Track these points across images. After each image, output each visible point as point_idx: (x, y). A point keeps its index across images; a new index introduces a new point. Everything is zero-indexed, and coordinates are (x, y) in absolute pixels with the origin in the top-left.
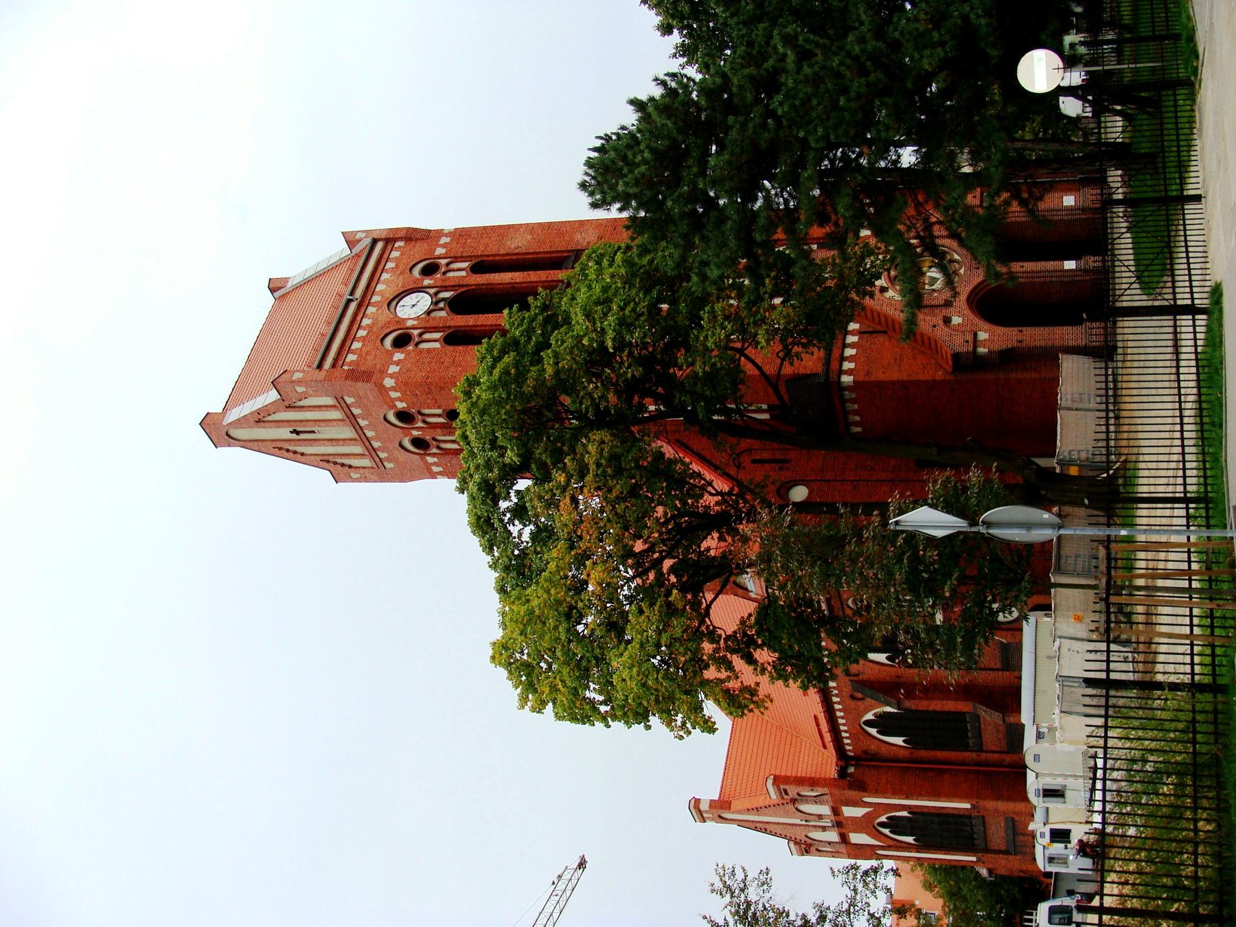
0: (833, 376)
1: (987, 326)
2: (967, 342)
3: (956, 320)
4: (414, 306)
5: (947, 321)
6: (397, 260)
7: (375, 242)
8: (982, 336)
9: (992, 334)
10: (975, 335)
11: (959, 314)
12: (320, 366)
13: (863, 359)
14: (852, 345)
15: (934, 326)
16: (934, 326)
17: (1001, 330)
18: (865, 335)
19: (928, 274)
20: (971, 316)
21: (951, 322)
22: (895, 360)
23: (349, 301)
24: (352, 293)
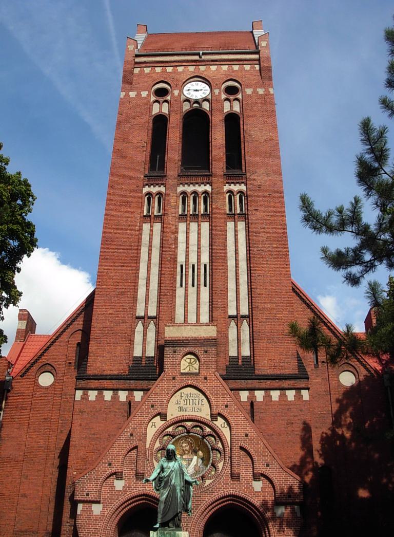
0: (83, 383)
1: (108, 513)
2: (88, 495)
3: (119, 485)
4: (197, 90)
5: (118, 475)
7: (258, 53)
8: (97, 509)
9: (97, 519)
10: (98, 502)
11: (127, 487)
12: (137, 56)
13: (97, 406)
14: (115, 397)
15: (110, 464)
16: (110, 464)
18: (126, 407)
19: (195, 458)
20: (122, 499)
21: (117, 479)
22: (94, 434)
23: (198, 54)
24: (203, 54)
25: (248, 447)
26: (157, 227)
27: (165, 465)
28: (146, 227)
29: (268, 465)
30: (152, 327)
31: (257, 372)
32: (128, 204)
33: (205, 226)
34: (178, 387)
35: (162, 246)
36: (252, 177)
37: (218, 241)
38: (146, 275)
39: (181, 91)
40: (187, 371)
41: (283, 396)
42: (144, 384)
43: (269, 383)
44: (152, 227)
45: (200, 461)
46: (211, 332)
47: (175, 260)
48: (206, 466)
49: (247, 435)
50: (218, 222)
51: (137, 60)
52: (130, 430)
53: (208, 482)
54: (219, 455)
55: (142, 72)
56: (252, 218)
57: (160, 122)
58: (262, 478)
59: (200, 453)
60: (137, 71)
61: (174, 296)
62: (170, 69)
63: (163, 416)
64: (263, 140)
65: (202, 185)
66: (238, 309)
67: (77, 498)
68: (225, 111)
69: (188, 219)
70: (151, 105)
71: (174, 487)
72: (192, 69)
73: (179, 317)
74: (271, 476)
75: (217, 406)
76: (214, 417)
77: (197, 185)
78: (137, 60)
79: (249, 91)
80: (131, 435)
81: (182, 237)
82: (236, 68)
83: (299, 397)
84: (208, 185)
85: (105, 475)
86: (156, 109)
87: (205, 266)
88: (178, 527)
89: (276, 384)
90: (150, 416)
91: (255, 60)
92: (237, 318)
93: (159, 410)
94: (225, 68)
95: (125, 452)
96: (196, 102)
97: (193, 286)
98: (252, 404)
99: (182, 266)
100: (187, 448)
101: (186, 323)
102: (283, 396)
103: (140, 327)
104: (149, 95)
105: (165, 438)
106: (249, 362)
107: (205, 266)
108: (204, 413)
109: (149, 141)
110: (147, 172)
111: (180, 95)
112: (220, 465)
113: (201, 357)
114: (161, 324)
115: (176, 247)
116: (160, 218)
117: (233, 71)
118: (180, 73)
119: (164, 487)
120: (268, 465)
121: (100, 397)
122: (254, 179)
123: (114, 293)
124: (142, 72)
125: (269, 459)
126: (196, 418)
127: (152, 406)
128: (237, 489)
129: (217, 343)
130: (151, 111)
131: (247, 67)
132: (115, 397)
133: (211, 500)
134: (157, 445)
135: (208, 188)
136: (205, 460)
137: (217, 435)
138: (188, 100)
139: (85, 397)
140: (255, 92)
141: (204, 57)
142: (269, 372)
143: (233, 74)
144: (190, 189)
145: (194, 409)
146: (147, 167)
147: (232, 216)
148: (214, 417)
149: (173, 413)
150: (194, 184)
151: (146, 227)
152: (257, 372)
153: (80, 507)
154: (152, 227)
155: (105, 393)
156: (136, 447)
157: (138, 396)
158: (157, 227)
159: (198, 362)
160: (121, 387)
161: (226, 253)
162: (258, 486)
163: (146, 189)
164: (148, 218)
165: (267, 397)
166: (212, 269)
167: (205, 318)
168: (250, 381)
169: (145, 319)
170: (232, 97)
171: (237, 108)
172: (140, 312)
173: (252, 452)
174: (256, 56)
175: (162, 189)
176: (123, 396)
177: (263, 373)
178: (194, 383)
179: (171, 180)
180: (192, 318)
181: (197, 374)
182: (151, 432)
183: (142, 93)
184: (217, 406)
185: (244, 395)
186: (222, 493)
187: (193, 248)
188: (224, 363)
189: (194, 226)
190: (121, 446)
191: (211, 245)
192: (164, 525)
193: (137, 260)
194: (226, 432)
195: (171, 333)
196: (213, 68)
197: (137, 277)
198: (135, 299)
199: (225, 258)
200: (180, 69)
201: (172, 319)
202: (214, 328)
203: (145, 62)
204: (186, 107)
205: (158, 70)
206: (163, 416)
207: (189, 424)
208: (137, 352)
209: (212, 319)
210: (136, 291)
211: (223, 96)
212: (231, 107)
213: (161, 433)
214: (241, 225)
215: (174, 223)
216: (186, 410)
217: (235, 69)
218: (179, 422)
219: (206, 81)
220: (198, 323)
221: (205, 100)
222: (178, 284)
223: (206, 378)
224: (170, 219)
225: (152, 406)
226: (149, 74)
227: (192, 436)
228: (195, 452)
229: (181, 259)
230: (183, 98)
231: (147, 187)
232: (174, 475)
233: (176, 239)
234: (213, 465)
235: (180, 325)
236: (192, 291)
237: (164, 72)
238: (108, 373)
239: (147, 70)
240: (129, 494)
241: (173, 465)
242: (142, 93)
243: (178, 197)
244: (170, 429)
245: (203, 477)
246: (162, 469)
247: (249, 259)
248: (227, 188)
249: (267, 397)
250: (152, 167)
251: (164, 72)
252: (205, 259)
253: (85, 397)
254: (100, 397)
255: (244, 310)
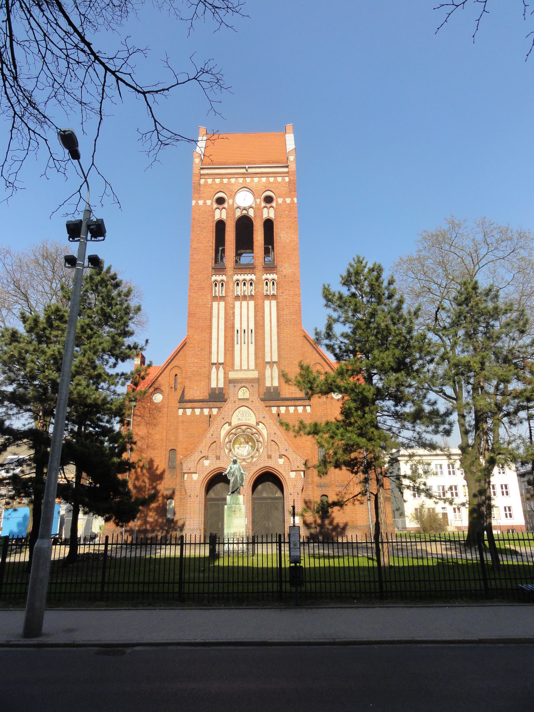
0: (183, 405)
1: (201, 478)
2: (190, 469)
3: (207, 463)
5: (206, 458)
6: (275, 182)
7: (287, 167)
8: (195, 477)
9: (195, 482)
10: (196, 473)
12: (202, 168)
13: (192, 418)
14: (202, 413)
15: (201, 452)
16: (201, 452)
17: (198, 486)
19: (247, 446)
24: (248, 168)
25: (276, 440)
26: (222, 304)
27: (232, 466)
28: (215, 304)
29: (286, 450)
30: (221, 369)
31: (281, 396)
32: (203, 289)
33: (252, 303)
34: (238, 407)
35: (225, 318)
36: (281, 270)
37: (260, 314)
38: (216, 337)
39: (234, 200)
40: (242, 397)
41: (296, 410)
42: (218, 404)
43: (288, 403)
44: (219, 304)
45: (250, 448)
46: (255, 375)
47: (233, 327)
48: (254, 450)
49: (275, 434)
50: (260, 301)
51: (203, 172)
52: (211, 432)
53: (255, 459)
54: (260, 445)
55: (206, 182)
56: (280, 299)
57: (220, 226)
58: (283, 457)
59: (250, 443)
60: (202, 181)
61: (233, 351)
62: (225, 181)
63: (230, 424)
64: (288, 241)
65: (249, 275)
66: (271, 359)
67: (184, 471)
68: (264, 217)
69: (241, 299)
70: (214, 212)
71: (237, 476)
72: (241, 180)
73: (237, 366)
74: (288, 456)
75: (259, 417)
76: (258, 424)
77: (246, 275)
78: (203, 172)
79: (280, 201)
80: (212, 435)
81: (237, 311)
82: (272, 180)
83: (305, 410)
84: (253, 275)
85: (199, 458)
86: (217, 217)
87: (252, 330)
88: (239, 493)
89: (292, 403)
90: (222, 424)
91: (285, 173)
92: (271, 363)
93: (227, 421)
94: (264, 180)
95: (209, 445)
96: (245, 209)
97: (245, 343)
98: (279, 415)
99: (238, 331)
100: (243, 441)
101: (241, 370)
102: (296, 410)
103: (214, 369)
104: (212, 204)
105: (231, 436)
106: (276, 390)
107: (252, 330)
108: (253, 421)
109: (214, 242)
110: (213, 265)
111: (233, 204)
112: (261, 450)
113: (250, 389)
114: (228, 368)
115: (234, 318)
116: (222, 298)
117: (270, 183)
118: (233, 184)
119: (232, 476)
120: (286, 450)
121: (193, 413)
122: (282, 271)
123: (197, 349)
124: (206, 182)
125: (287, 447)
126: (246, 424)
127: (223, 418)
128: (270, 463)
129: (259, 381)
130: (214, 217)
131: (279, 179)
132: (202, 413)
133: (256, 469)
134: (227, 440)
135: (253, 277)
136: (253, 447)
137: (259, 433)
138: (238, 207)
139: (184, 413)
140: (284, 202)
141: (250, 171)
142: (288, 396)
143: (270, 186)
144: (241, 277)
145: (246, 419)
146: (214, 261)
147: (267, 296)
148: (258, 424)
149: (235, 422)
150: (244, 274)
151: (215, 304)
152: (281, 396)
153: (186, 476)
154: (219, 304)
155: (196, 410)
156: (215, 442)
157: (215, 411)
158: (222, 304)
159: (248, 392)
160: (205, 406)
161: (264, 322)
162: (281, 461)
163: (214, 278)
164: (215, 298)
165: (287, 411)
166: (255, 333)
167: (252, 366)
168: (277, 402)
169: (217, 365)
170: (268, 205)
171: (272, 216)
172: (214, 360)
173: (278, 443)
174: (286, 170)
175: (224, 278)
176: (206, 411)
177: (285, 397)
178: (246, 405)
179: (230, 271)
180: (245, 367)
181: (247, 399)
182: (223, 432)
183: (207, 201)
184: (259, 417)
185: (274, 410)
186: (262, 465)
187: (244, 319)
188: (262, 391)
189: (244, 303)
190: (207, 440)
191: (255, 317)
192: (233, 493)
193: (210, 327)
194: (265, 432)
195: (232, 375)
196: (256, 180)
197: (211, 338)
198: (210, 352)
199: (263, 326)
200: (233, 181)
201: (233, 365)
202: (257, 372)
203: (208, 174)
204: (238, 214)
205: (218, 181)
206: (230, 424)
207: (244, 427)
208: (213, 385)
209: (256, 365)
210: (210, 347)
211: (263, 204)
212: (268, 213)
213: (229, 433)
214: (274, 303)
215: (231, 302)
216: (242, 420)
217: (271, 181)
218: (238, 427)
219: (250, 190)
220: (248, 370)
221: (251, 207)
222: (236, 343)
223: (252, 402)
224: (230, 299)
225: (223, 418)
226: (211, 184)
227: (246, 434)
228: (247, 443)
229: (237, 326)
230: (235, 206)
231: (214, 276)
232: (236, 471)
233: (234, 313)
234: (257, 450)
235: (237, 371)
236: (244, 347)
237: (222, 182)
238: (196, 398)
239: (210, 181)
240: (212, 468)
241: (236, 466)
242: (207, 201)
243: (234, 284)
244: (233, 431)
245: (252, 457)
246: (231, 468)
247: (278, 326)
248: (265, 276)
249: (287, 411)
250: (216, 261)
251: (222, 182)
252: (252, 326)
253: (184, 413)
254: (193, 413)
255: (275, 359)
